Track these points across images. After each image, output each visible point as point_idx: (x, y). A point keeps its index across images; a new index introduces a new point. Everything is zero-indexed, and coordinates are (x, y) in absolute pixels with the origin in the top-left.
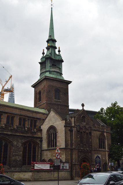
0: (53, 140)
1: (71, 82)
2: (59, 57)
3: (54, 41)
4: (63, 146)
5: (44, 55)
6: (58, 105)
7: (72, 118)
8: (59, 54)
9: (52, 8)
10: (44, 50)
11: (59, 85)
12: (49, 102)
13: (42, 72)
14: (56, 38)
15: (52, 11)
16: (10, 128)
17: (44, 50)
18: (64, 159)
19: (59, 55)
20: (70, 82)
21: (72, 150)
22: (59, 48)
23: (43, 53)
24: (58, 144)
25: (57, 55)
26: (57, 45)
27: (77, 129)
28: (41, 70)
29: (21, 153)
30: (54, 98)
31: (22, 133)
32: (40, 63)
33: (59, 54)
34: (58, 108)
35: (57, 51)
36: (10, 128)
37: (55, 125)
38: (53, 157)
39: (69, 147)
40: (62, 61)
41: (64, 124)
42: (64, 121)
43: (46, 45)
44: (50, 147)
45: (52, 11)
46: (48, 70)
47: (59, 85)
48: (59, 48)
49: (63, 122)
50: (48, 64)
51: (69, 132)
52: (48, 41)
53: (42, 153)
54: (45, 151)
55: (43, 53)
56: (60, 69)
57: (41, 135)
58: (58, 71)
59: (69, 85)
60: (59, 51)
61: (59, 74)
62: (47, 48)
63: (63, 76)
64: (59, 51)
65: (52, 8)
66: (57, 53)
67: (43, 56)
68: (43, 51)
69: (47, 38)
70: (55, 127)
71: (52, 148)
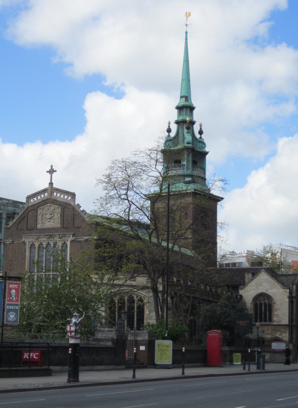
0: (265, 313)
1: (222, 199)
2: (202, 144)
3: (192, 109)
4: (285, 321)
5: (173, 134)
8: (201, 138)
9: (186, 33)
10: (169, 124)
14: (194, 102)
15: (186, 39)
17: (169, 124)
18: (285, 338)
20: (218, 199)
22: (201, 126)
23: (169, 131)
24: (275, 319)
25: (197, 139)
26: (197, 116)
33: (201, 138)
35: (196, 129)
37: (270, 292)
38: (266, 335)
40: (206, 153)
41: (288, 294)
43: (174, 116)
44: (259, 321)
45: (186, 39)
48: (201, 126)
52: (180, 108)
55: (169, 131)
56: (204, 170)
58: (202, 175)
59: (219, 203)
61: (204, 181)
62: (177, 122)
64: (201, 132)
65: (186, 33)
66: (198, 136)
67: (169, 136)
68: (169, 126)
70: (270, 296)
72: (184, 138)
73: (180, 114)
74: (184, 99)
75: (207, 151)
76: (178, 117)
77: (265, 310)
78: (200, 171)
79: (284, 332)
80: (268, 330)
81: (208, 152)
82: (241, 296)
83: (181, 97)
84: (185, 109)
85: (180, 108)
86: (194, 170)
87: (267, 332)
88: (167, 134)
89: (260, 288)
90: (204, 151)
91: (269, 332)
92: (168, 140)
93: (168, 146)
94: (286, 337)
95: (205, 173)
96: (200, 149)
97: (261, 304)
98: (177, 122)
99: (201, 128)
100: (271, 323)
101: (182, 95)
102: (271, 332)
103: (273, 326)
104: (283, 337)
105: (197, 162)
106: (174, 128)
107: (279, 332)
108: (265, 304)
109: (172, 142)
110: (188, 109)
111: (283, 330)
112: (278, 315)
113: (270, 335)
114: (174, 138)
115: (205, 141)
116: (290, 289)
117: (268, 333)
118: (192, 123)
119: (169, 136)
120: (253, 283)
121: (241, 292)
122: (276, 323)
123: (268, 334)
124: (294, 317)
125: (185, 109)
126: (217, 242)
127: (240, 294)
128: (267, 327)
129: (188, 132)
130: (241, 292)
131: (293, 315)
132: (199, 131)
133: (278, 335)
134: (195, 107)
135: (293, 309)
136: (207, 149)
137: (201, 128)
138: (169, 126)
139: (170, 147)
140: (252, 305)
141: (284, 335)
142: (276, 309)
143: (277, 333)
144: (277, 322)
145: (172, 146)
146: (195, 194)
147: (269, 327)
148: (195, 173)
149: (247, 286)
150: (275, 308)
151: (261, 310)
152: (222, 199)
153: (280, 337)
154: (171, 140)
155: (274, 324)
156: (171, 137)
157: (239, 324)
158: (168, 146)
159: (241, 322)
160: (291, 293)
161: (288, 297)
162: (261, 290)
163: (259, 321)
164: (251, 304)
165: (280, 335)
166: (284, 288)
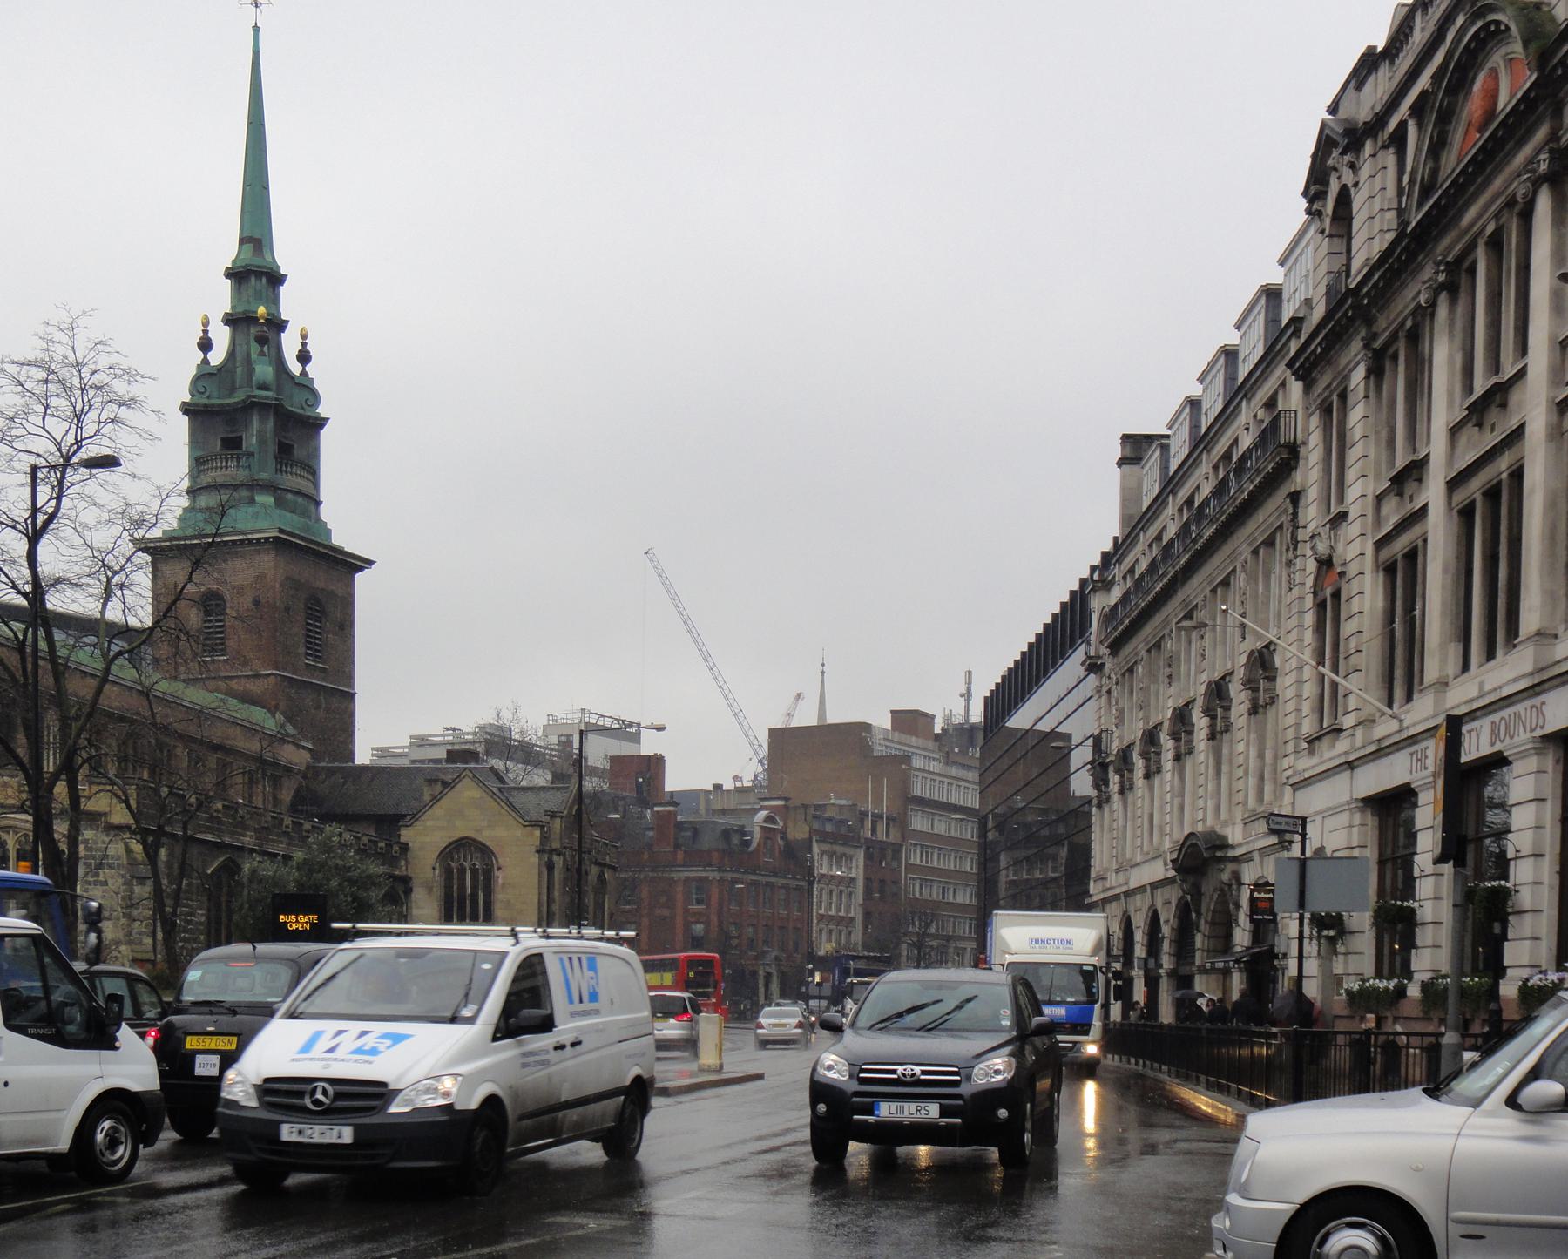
0: (474, 896)
3: (275, 279)
5: (217, 357)
10: (206, 323)
11: (320, 579)
13: (206, 479)
17: (206, 323)
19: (306, 387)
22: (304, 336)
23: (205, 345)
25: (291, 377)
26: (291, 303)
27: (565, 860)
30: (302, 650)
33: (304, 373)
34: (318, 708)
35: (290, 344)
37: (485, 837)
42: (538, 833)
43: (220, 298)
44: (455, 920)
47: (320, 579)
48: (304, 336)
49: (532, 835)
50: (256, 433)
55: (205, 345)
62: (229, 320)
63: (325, 513)
64: (304, 357)
65: (256, 29)
66: (295, 368)
67: (205, 361)
69: (228, 250)
72: (250, 371)
74: (249, 247)
75: (322, 416)
76: (233, 307)
77: (474, 887)
78: (300, 476)
81: (328, 419)
82: (405, 848)
83: (242, 241)
84: (253, 279)
85: (238, 275)
86: (281, 471)
88: (201, 355)
89: (458, 823)
90: (313, 415)
92: (205, 377)
93: (203, 393)
96: (303, 408)
97: (462, 871)
98: (229, 320)
99: (304, 344)
101: (245, 235)
105: (292, 446)
106: (222, 337)
108: (474, 871)
110: (264, 280)
114: (220, 369)
115: (316, 385)
118: (280, 326)
119: (205, 361)
120: (438, 810)
121: (406, 835)
125: (253, 279)
127: (403, 839)
129: (262, 354)
130: (406, 835)
131: (554, 901)
132: (300, 351)
134: (286, 276)
136: (322, 411)
137: (304, 344)
138: (206, 332)
139: (208, 397)
140: (437, 872)
145: (215, 394)
146: (280, 544)
149: (423, 818)
151: (462, 886)
154: (211, 374)
156: (212, 364)
157: (286, 923)
158: (203, 393)
159: (293, 917)
160: (544, 838)
162: (461, 830)
163: (455, 920)
164: (434, 869)
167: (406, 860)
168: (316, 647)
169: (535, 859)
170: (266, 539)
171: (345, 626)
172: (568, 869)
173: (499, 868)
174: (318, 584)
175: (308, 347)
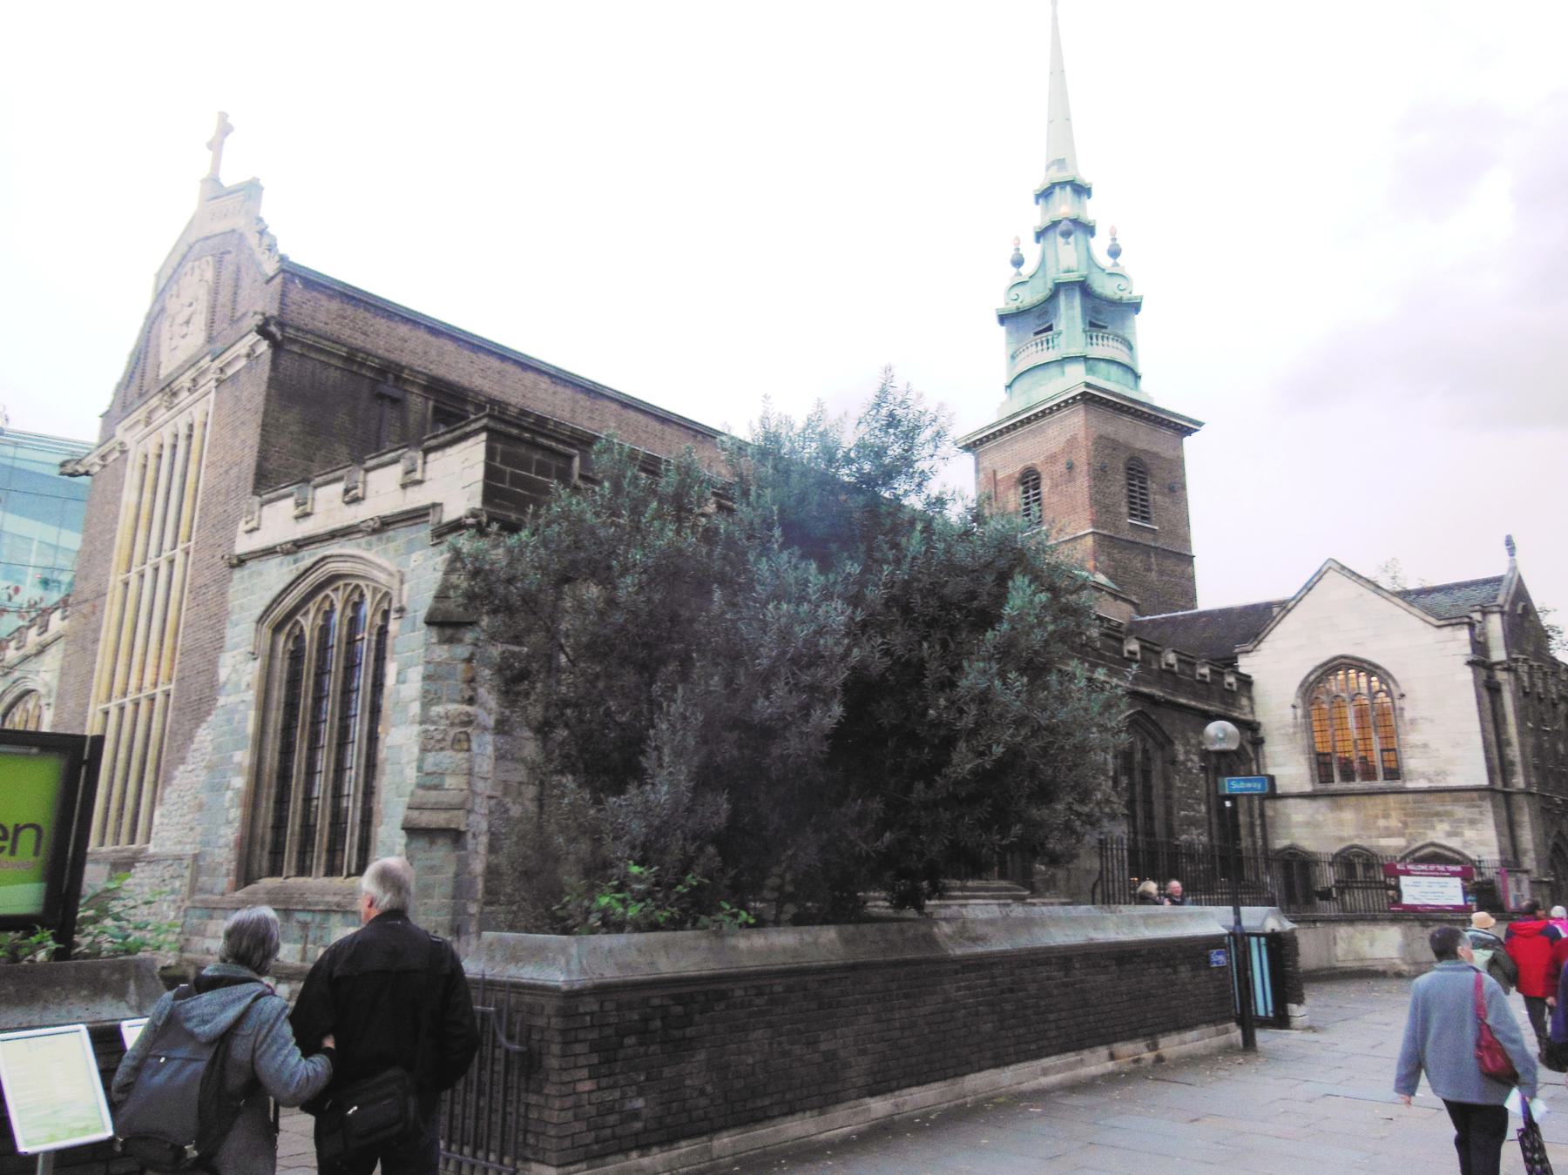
2: (1118, 280)
3: (1081, 190)
6: (1147, 550)
7: (1485, 613)
11: (1142, 439)
12: (1105, 532)
15: (1055, 19)
16: (1155, 667)
20: (1182, 428)
21: (1508, 796)
22: (1113, 232)
23: (1018, 262)
28: (1013, 357)
29: (1203, 808)
30: (1125, 510)
31: (1196, 696)
32: (1003, 319)
33: (1116, 265)
34: (1149, 570)
36: (1155, 667)
39: (1499, 785)
40: (1136, 307)
44: (1337, 777)
45: (1055, 19)
46: (1074, 352)
48: (1113, 232)
51: (1485, 693)
52: (1045, 194)
53: (1269, 813)
54: (1291, 801)
55: (1018, 262)
57: (1252, 711)
59: (1187, 440)
60: (1115, 253)
61: (1130, 377)
64: (1115, 253)
66: (1105, 261)
71: (1380, 783)
73: (1046, 210)
79: (1472, 822)
80: (1386, 816)
82: (1246, 682)
87: (1382, 823)
88: (1014, 270)
91: (1394, 822)
94: (1482, 843)
95: (1132, 357)
99: (1114, 239)
100: (1397, 784)
102: (1405, 824)
103: (1410, 797)
104: (1466, 844)
107: (1441, 821)
109: (1027, 286)
110: (1068, 188)
111: (1460, 811)
112: (1425, 746)
113: (1401, 834)
115: (1128, 271)
116: (1471, 626)
117: (1387, 828)
122: (1423, 784)
123: (1389, 833)
124: (1514, 752)
126: (1194, 553)
128: (1379, 800)
130: (1245, 665)
131: (1509, 744)
133: (1439, 834)
135: (1504, 717)
141: (1469, 834)
142: (1413, 721)
143: (1433, 828)
144: (1424, 776)
146: (1090, 399)
147: (1392, 799)
148: (1099, 350)
150: (1408, 715)
152: (1200, 424)
153: (1454, 843)
155: (1410, 785)
160: (1480, 646)
161: (1470, 663)
165: (1450, 835)
166: (1439, 627)
167: (1251, 699)
168: (1139, 506)
169: (1467, 674)
170: (1074, 398)
171: (1176, 489)
172: (1526, 694)
173: (1402, 696)
174: (1138, 445)
175: (1118, 242)
